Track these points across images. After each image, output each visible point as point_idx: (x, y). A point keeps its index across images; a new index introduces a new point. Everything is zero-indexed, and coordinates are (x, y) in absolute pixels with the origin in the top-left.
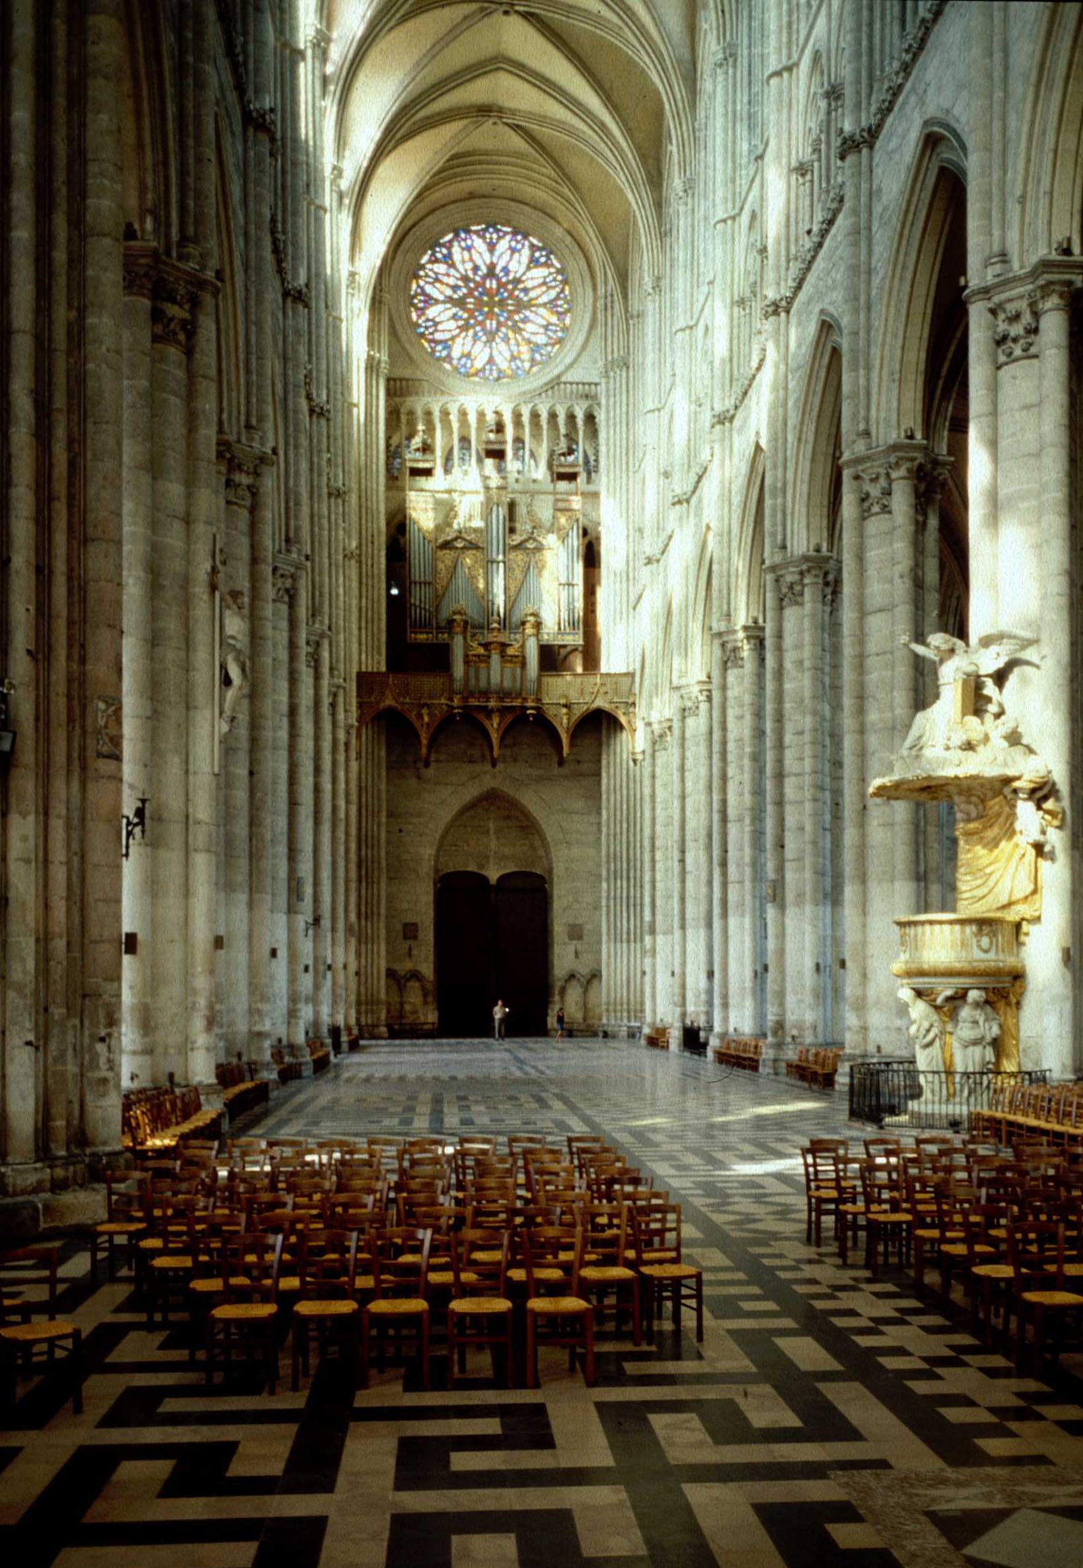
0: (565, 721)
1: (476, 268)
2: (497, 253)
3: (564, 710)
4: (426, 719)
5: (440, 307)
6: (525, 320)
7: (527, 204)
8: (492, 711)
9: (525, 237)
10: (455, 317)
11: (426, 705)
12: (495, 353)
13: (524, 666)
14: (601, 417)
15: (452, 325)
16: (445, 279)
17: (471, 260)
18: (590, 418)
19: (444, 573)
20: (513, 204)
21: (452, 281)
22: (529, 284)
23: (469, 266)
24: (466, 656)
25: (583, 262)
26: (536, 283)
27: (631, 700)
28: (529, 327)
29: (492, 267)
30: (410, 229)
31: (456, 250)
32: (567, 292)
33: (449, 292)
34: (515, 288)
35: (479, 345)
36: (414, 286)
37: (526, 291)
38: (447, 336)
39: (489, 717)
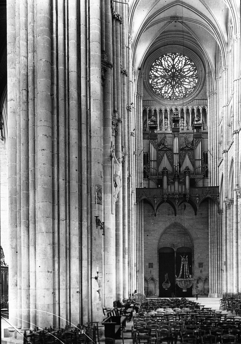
0: (198, 201)
4: (156, 202)
8: (175, 199)
13: (185, 184)
14: (208, 110)
18: (204, 110)
29: (173, 66)
34: (181, 72)
37: (184, 72)
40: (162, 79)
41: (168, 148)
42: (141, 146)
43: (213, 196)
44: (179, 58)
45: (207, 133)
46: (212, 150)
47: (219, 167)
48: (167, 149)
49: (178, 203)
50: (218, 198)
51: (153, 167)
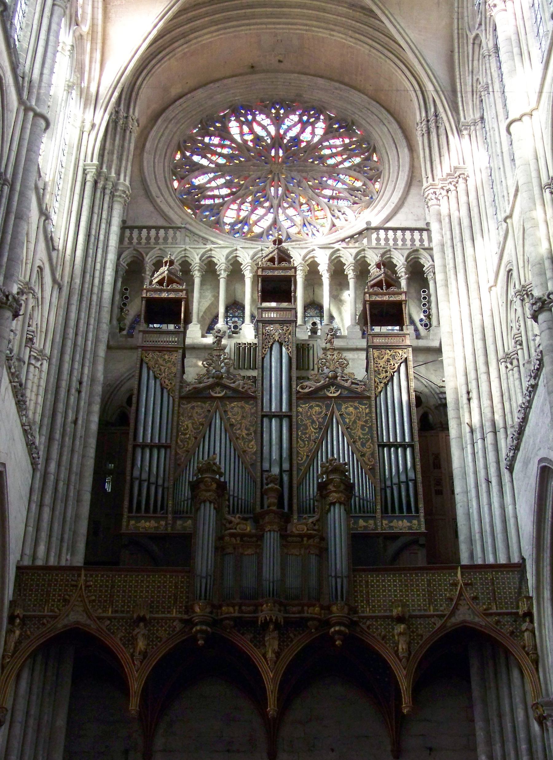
0: (402, 646)
1: (258, 139)
2: (284, 127)
3: (401, 627)
4: (141, 644)
5: (212, 175)
6: (323, 186)
7: (322, 77)
8: (266, 624)
9: (319, 110)
10: (228, 185)
11: (142, 619)
12: (282, 217)
15: (225, 191)
16: (219, 150)
17: (252, 131)
19: (191, 432)
20: (304, 77)
21: (225, 151)
22: (326, 152)
23: (249, 137)
24: (220, 538)
25: (395, 126)
26: (334, 151)
27: (523, 609)
28: (328, 192)
30: (175, 101)
31: (234, 127)
32: (375, 158)
33: (222, 161)
35: (260, 211)
36: (178, 156)
37: (322, 159)
38: (217, 201)
39: (260, 643)
40: (228, 178)
41: (234, 390)
42: (93, 380)
43: (492, 620)
44: (301, 116)
45: (438, 351)
46: (469, 400)
47: (511, 469)
48: (230, 393)
49: (278, 654)
50: (524, 627)
51: (145, 476)
